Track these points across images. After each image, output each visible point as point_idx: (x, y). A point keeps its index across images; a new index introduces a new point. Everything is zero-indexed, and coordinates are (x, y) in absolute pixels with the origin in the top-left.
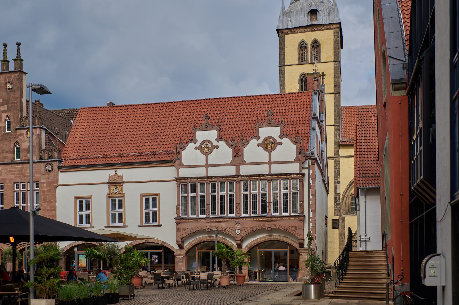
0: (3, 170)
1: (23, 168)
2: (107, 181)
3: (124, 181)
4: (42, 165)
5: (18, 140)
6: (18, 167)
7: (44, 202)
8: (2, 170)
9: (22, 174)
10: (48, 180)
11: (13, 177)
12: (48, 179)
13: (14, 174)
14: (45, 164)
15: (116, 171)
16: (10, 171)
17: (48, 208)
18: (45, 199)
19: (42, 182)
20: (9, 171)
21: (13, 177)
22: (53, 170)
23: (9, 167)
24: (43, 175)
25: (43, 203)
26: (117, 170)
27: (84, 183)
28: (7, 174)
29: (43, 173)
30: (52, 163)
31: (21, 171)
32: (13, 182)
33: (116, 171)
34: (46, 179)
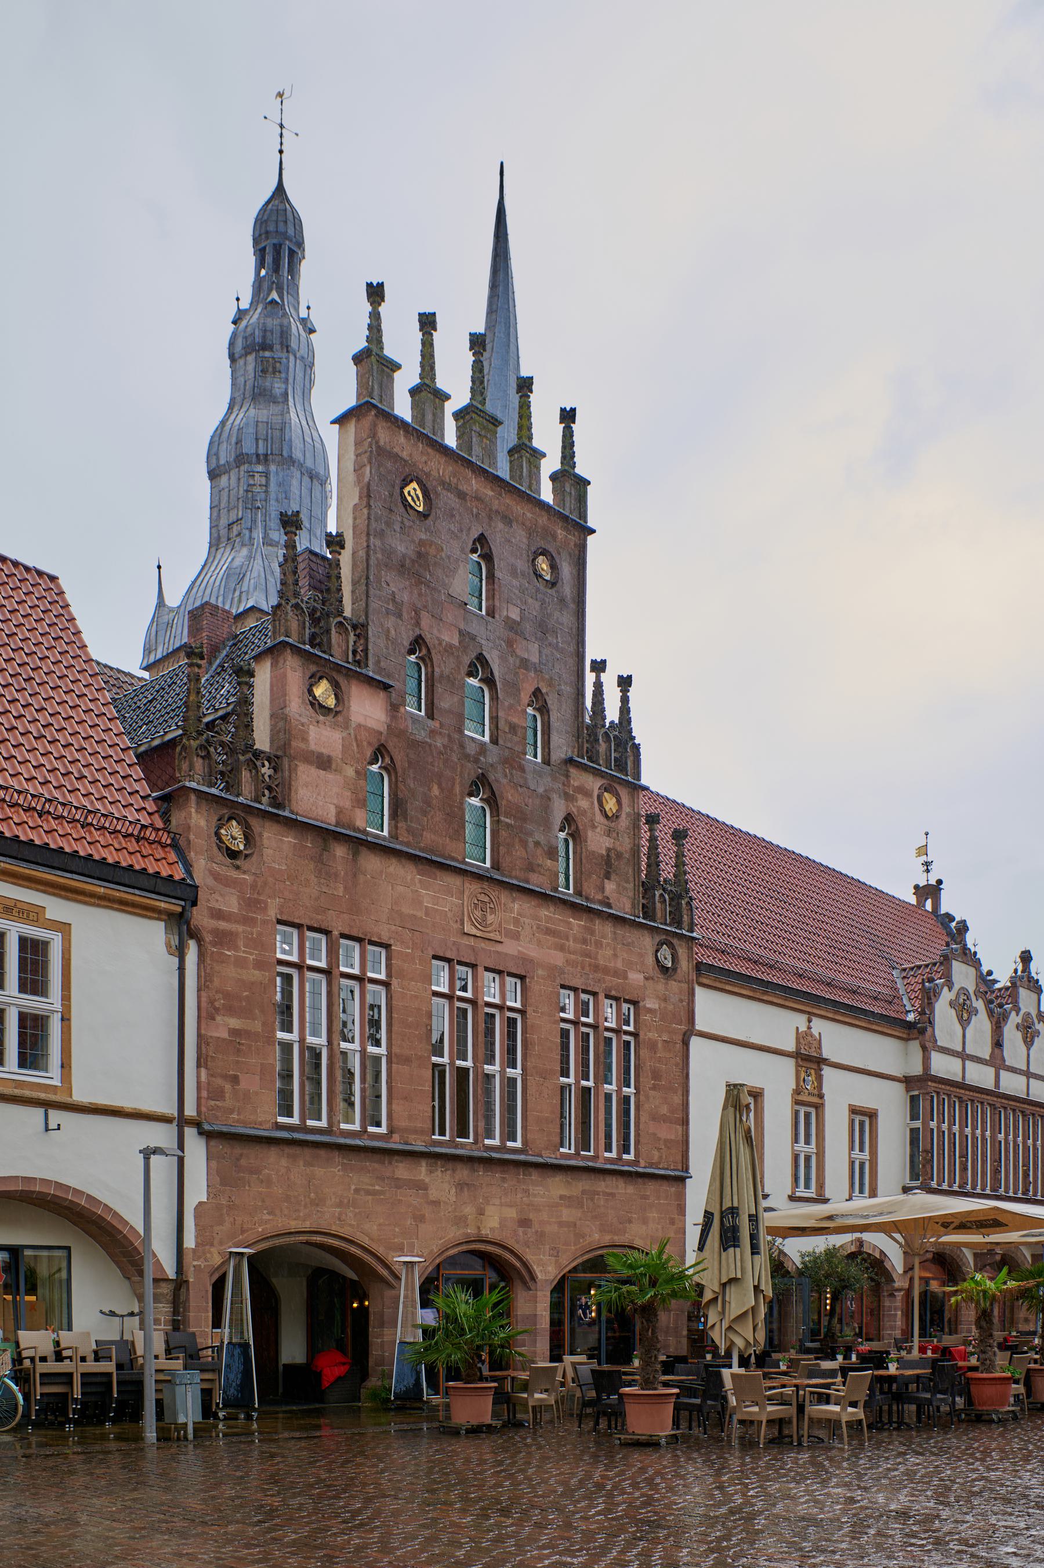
0: (527, 921)
1: (592, 932)
2: (790, 1046)
3: (825, 1056)
4: (647, 942)
5: (574, 810)
6: (577, 924)
7: (654, 1088)
8: (522, 920)
9: (590, 957)
10: (663, 1005)
11: (558, 958)
12: (665, 1000)
13: (562, 948)
14: (658, 939)
15: (810, 1021)
16: (548, 932)
17: (664, 1110)
18: (656, 1075)
19: (648, 1006)
20: (547, 928)
21: (558, 958)
22: (679, 971)
23: (547, 913)
24: (651, 981)
25: (650, 1089)
26: (814, 1019)
27: (751, 1041)
28: (539, 942)
29: (651, 973)
30: (675, 941)
31: (584, 941)
32: (558, 981)
33: (810, 1021)
34: (658, 997)
